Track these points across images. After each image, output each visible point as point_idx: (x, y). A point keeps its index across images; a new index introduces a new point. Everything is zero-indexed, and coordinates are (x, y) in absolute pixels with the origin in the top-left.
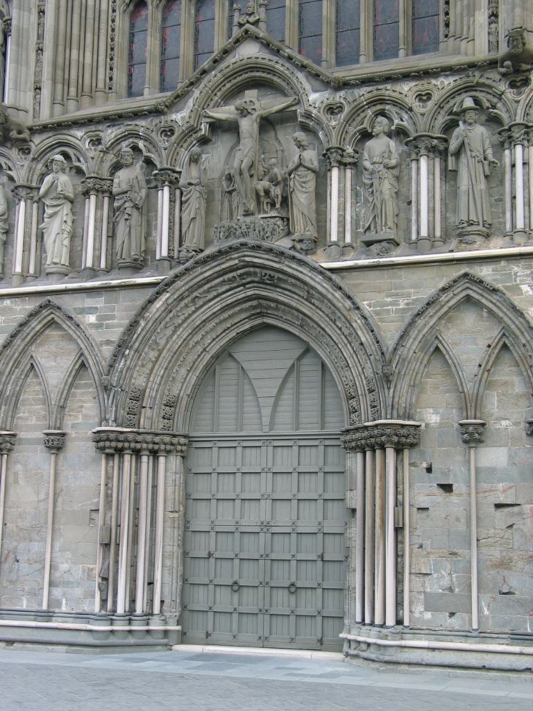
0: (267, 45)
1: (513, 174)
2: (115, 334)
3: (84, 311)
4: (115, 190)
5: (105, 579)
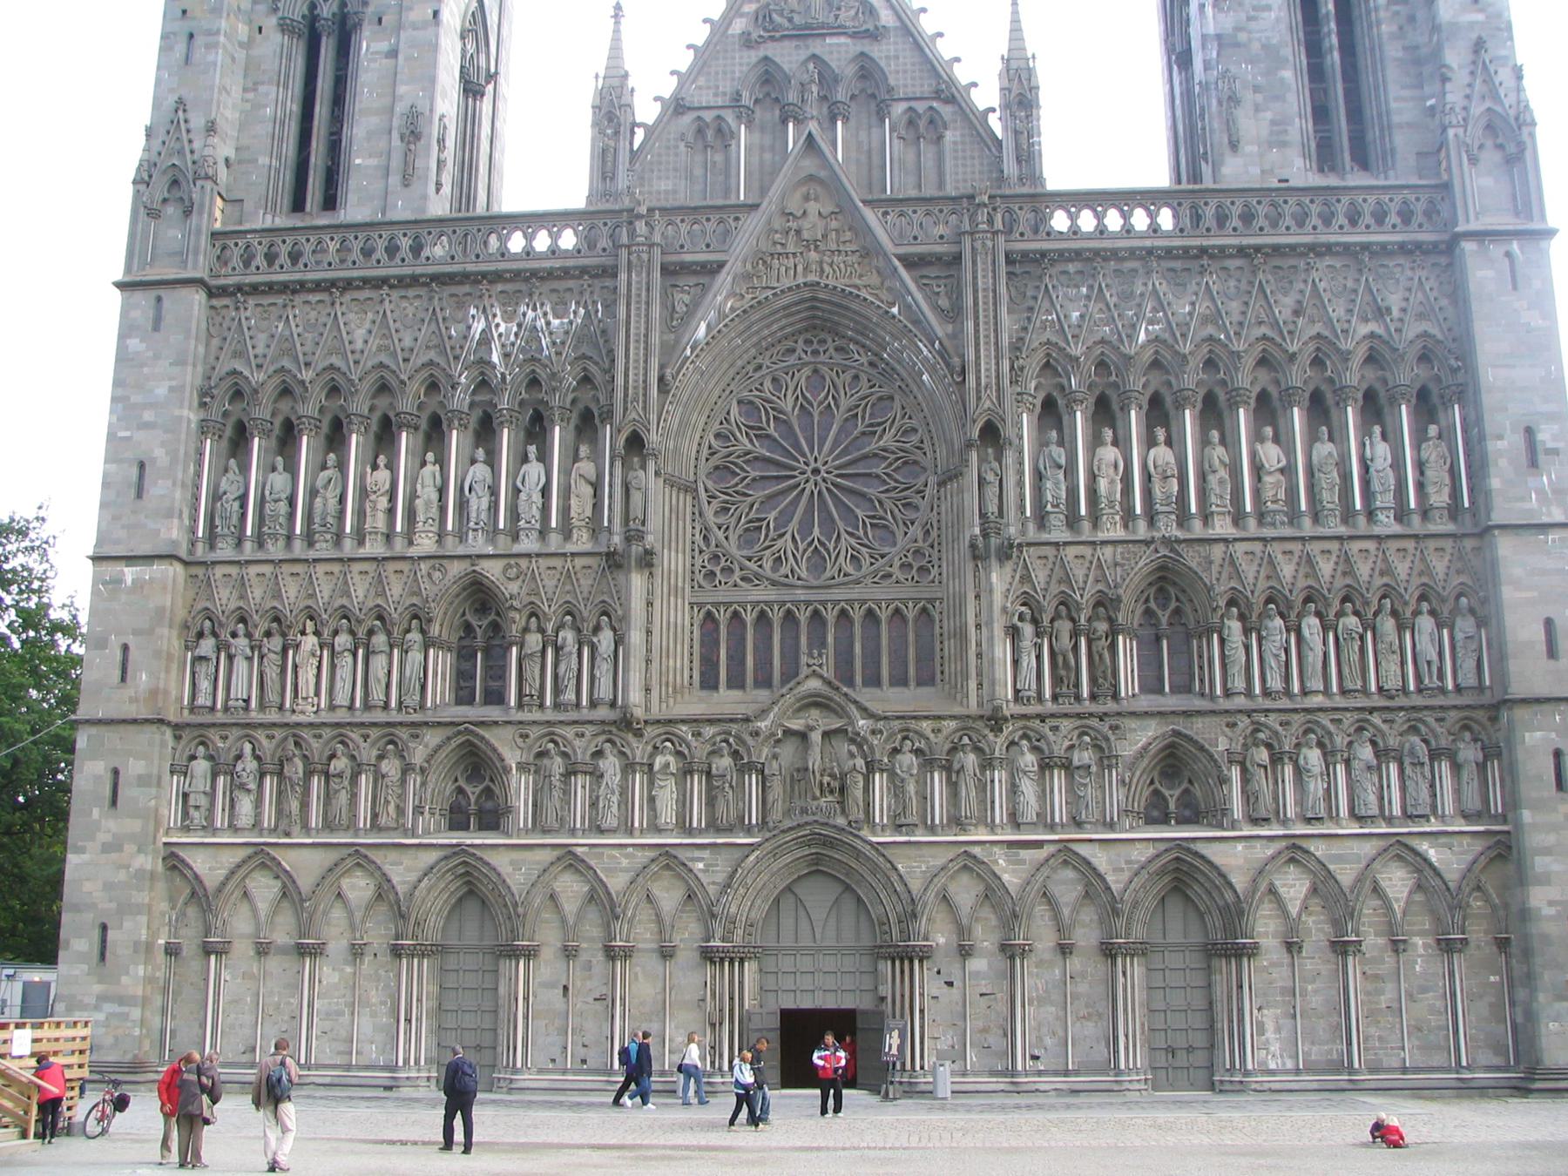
0: (829, 683)
2: (721, 878)
4: (714, 771)
5: (713, 1048)
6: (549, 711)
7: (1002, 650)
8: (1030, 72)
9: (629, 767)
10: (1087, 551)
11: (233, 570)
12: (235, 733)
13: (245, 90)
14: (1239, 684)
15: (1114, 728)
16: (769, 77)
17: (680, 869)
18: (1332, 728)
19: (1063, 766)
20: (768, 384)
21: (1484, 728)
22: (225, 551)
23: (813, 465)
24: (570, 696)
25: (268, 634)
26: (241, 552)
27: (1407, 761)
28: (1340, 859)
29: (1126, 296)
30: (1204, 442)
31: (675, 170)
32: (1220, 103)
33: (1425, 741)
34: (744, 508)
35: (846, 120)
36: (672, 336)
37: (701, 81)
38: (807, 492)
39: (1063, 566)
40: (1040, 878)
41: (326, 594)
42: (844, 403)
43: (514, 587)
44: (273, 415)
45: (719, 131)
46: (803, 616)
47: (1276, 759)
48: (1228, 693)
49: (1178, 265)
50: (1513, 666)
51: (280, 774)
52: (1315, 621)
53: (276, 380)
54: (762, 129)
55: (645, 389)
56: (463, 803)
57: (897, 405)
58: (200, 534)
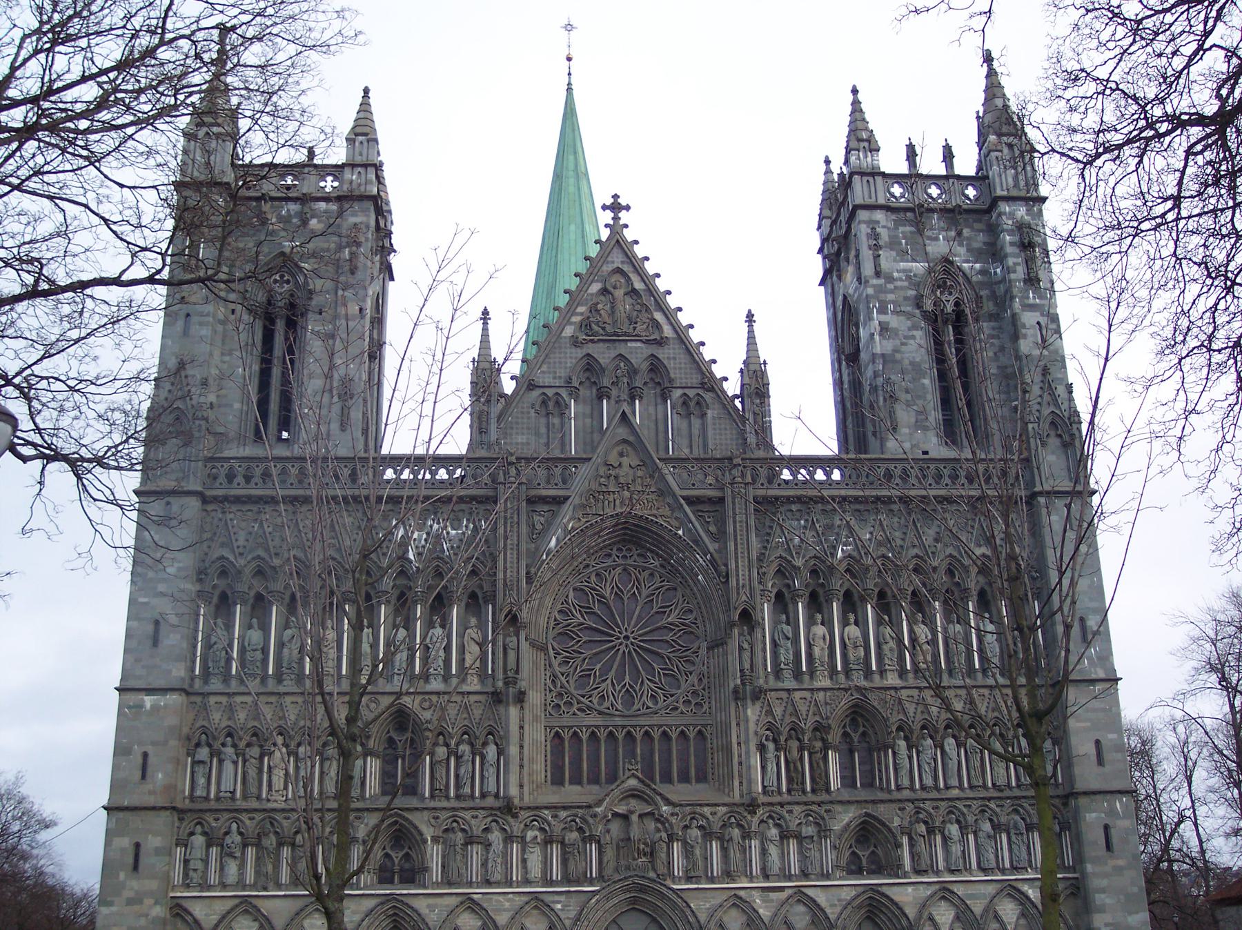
1: (751, 851)
2: (572, 914)
3: (554, 902)
4: (567, 841)
6: (452, 801)
7: (756, 761)
8: (763, 374)
9: (508, 839)
10: (807, 694)
11: (224, 699)
12: (227, 816)
13: (223, 354)
14: (906, 782)
15: (827, 811)
16: (590, 366)
17: (546, 909)
18: (965, 810)
19: (796, 837)
20: (593, 578)
21: (1059, 811)
22: (216, 685)
23: (625, 633)
24: (467, 790)
25: (249, 745)
26: (229, 686)
27: (1012, 832)
28: (972, 897)
29: (829, 527)
30: (879, 622)
31: (528, 428)
32: (885, 400)
33: (1023, 819)
34: (579, 661)
35: (641, 398)
36: (533, 545)
37: (544, 368)
38: (621, 652)
39: (793, 705)
40: (783, 911)
41: (293, 717)
42: (645, 592)
43: (427, 715)
44: (249, 588)
45: (557, 403)
46: (620, 736)
47: (931, 831)
48: (899, 788)
49: (861, 507)
50: (1077, 771)
51: (258, 845)
52: (952, 741)
53: (254, 564)
54: (585, 402)
55: (518, 581)
56: (389, 864)
57: (679, 594)
58: (197, 673)
